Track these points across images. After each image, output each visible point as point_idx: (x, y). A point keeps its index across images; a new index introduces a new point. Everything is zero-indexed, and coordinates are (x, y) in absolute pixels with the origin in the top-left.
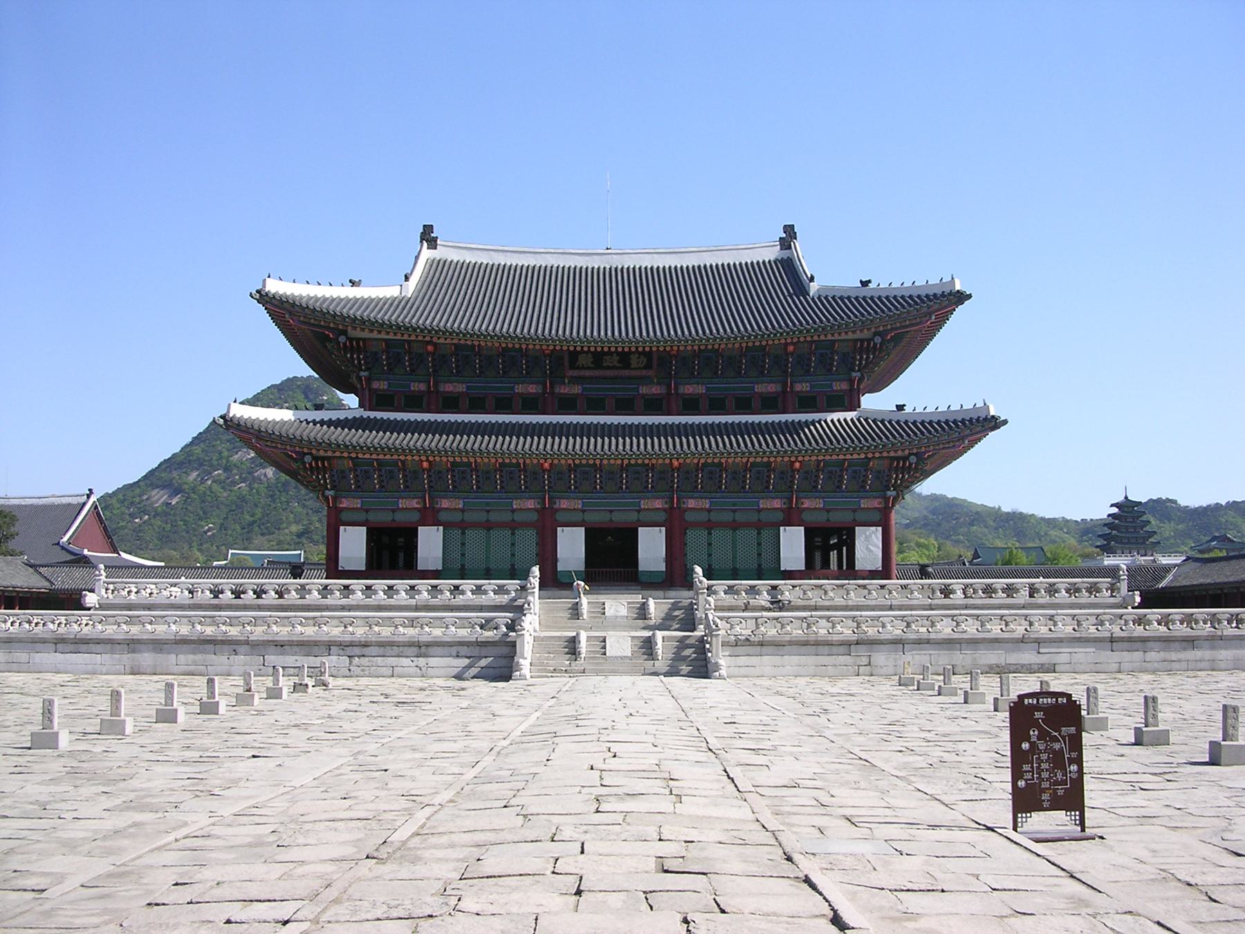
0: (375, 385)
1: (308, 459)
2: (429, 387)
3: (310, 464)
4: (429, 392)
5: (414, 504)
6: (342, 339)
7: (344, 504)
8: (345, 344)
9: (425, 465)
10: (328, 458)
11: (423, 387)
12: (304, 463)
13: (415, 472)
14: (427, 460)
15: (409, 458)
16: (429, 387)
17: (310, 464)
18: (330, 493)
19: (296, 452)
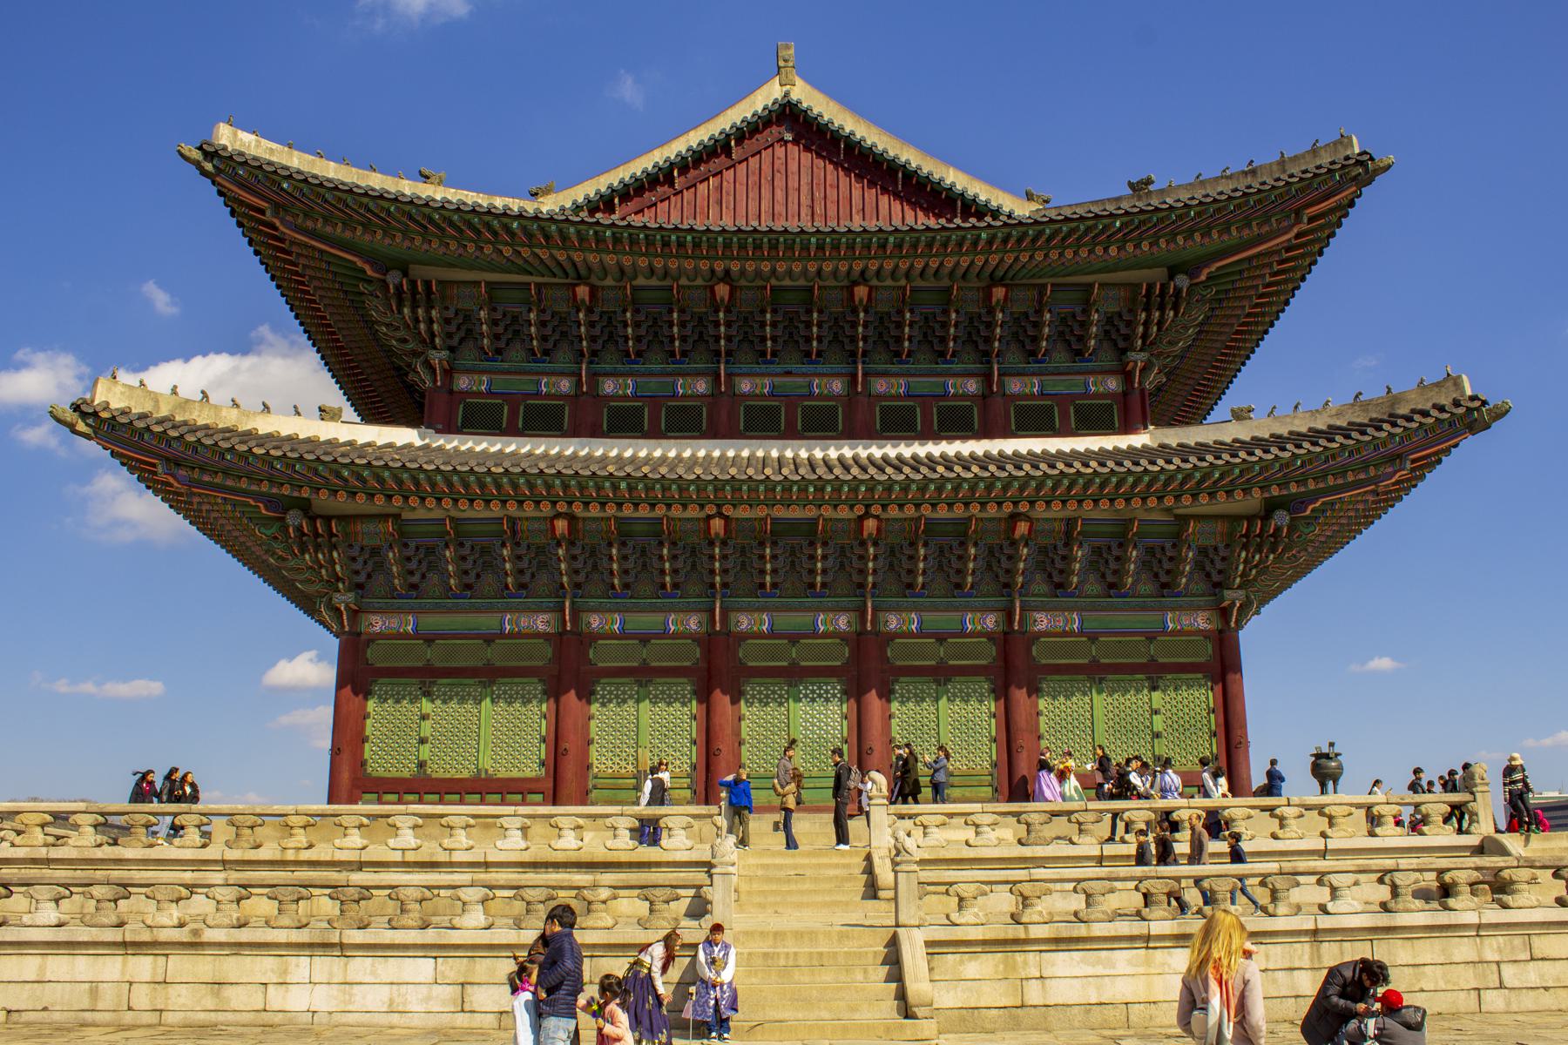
0: (463, 383)
1: (294, 518)
2: (579, 384)
3: (299, 529)
4: (575, 397)
5: (542, 622)
6: (393, 278)
7: (377, 623)
8: (399, 288)
9: (561, 525)
10: (342, 518)
11: (565, 385)
12: (285, 529)
13: (541, 550)
14: (571, 518)
15: (529, 510)
16: (579, 384)
17: (299, 529)
18: (344, 599)
19: (270, 501)
